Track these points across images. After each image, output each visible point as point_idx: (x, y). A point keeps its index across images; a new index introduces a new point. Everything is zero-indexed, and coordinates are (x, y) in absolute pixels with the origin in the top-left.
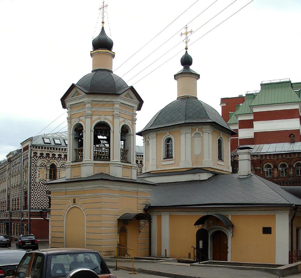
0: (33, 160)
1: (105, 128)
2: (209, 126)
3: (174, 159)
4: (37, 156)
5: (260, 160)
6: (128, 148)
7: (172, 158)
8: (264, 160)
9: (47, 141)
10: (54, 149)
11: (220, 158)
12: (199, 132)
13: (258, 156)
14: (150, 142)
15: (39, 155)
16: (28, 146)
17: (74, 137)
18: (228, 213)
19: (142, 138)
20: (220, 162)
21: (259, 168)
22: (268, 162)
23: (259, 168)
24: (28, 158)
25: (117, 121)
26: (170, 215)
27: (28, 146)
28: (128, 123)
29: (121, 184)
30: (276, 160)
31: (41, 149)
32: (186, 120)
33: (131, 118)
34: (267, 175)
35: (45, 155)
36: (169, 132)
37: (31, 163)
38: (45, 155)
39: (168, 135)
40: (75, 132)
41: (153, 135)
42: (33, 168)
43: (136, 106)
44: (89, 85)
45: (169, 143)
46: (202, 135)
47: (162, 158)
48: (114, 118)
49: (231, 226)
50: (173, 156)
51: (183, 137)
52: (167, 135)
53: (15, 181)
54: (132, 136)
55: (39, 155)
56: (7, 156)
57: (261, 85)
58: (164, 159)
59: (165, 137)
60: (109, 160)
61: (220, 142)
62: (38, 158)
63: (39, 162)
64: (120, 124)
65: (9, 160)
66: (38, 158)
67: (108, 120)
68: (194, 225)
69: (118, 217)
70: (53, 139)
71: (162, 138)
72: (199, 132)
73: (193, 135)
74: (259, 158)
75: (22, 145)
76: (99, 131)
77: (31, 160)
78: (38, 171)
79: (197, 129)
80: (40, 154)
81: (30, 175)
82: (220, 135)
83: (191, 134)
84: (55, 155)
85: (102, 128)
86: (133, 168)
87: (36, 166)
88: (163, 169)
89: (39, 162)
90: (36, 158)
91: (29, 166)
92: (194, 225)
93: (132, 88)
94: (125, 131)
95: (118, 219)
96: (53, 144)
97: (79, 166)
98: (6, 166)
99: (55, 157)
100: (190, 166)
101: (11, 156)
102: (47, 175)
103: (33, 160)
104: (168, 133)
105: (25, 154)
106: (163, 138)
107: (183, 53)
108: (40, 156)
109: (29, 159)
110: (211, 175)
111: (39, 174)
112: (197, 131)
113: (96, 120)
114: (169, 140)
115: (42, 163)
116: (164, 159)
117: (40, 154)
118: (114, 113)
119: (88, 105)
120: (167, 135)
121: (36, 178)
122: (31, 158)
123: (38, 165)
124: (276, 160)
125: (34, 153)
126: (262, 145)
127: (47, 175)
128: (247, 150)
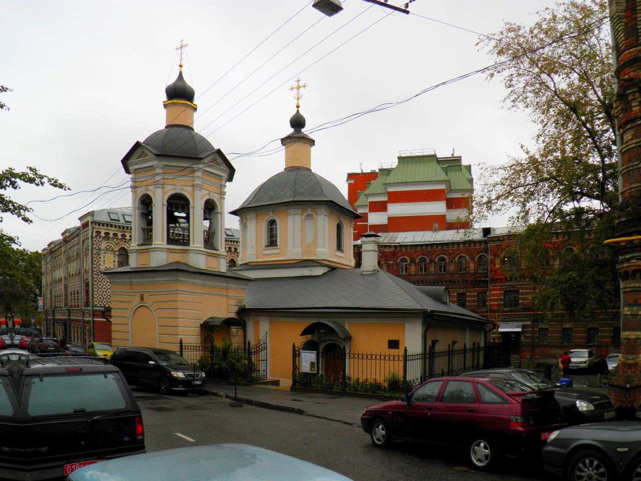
0: (95, 241)
1: (182, 202)
3: (279, 247)
4: (100, 236)
5: (394, 252)
6: (215, 230)
7: (276, 245)
9: (113, 216)
10: (123, 228)
14: (248, 224)
15: (103, 235)
16: (88, 222)
17: (140, 211)
19: (238, 218)
20: (339, 253)
21: (392, 262)
22: (404, 255)
23: (392, 262)
24: (88, 238)
25: (198, 193)
27: (88, 222)
28: (215, 198)
30: (413, 253)
31: (105, 227)
32: (296, 198)
33: (218, 190)
34: (402, 272)
35: (111, 235)
36: (273, 212)
37: (92, 244)
38: (111, 235)
39: (271, 215)
40: (141, 206)
41: (251, 216)
42: (95, 252)
43: (225, 176)
44: (160, 144)
45: (273, 227)
46: (315, 216)
47: (264, 246)
48: (194, 190)
50: (278, 243)
51: (290, 219)
52: (269, 216)
53: (73, 267)
54: (220, 215)
55: (103, 235)
56: (63, 234)
58: (266, 246)
59: (269, 218)
60: (188, 244)
61: (339, 227)
62: (101, 239)
63: (103, 244)
64: (203, 197)
65: (66, 240)
66: (101, 239)
67: (187, 192)
70: (123, 215)
71: (264, 219)
72: (312, 213)
73: (303, 217)
74: (392, 249)
75: (81, 221)
76: (174, 205)
77: (92, 241)
78: (102, 257)
79: (309, 210)
80: (105, 233)
81: (92, 261)
83: (302, 215)
84: (125, 236)
85: (178, 203)
86: (221, 256)
87: (99, 249)
88: (265, 260)
89: (104, 245)
90: (100, 238)
91: (90, 248)
93: (219, 152)
94: (210, 208)
96: (122, 221)
97: (147, 251)
98: (61, 247)
99: (126, 239)
100: (300, 257)
101: (68, 234)
102: (114, 261)
103: (95, 241)
104: (271, 213)
105: (84, 232)
106: (266, 219)
108: (104, 237)
109: (90, 239)
110: (327, 269)
111: (104, 260)
113: (170, 191)
114: (272, 223)
115: (108, 246)
116: (266, 246)
117: (105, 233)
118: (194, 183)
119: (158, 171)
120: (269, 216)
121: (100, 265)
122: (92, 238)
123: (102, 248)
125: (97, 232)
126: (397, 233)
127: (114, 261)
128: (373, 239)
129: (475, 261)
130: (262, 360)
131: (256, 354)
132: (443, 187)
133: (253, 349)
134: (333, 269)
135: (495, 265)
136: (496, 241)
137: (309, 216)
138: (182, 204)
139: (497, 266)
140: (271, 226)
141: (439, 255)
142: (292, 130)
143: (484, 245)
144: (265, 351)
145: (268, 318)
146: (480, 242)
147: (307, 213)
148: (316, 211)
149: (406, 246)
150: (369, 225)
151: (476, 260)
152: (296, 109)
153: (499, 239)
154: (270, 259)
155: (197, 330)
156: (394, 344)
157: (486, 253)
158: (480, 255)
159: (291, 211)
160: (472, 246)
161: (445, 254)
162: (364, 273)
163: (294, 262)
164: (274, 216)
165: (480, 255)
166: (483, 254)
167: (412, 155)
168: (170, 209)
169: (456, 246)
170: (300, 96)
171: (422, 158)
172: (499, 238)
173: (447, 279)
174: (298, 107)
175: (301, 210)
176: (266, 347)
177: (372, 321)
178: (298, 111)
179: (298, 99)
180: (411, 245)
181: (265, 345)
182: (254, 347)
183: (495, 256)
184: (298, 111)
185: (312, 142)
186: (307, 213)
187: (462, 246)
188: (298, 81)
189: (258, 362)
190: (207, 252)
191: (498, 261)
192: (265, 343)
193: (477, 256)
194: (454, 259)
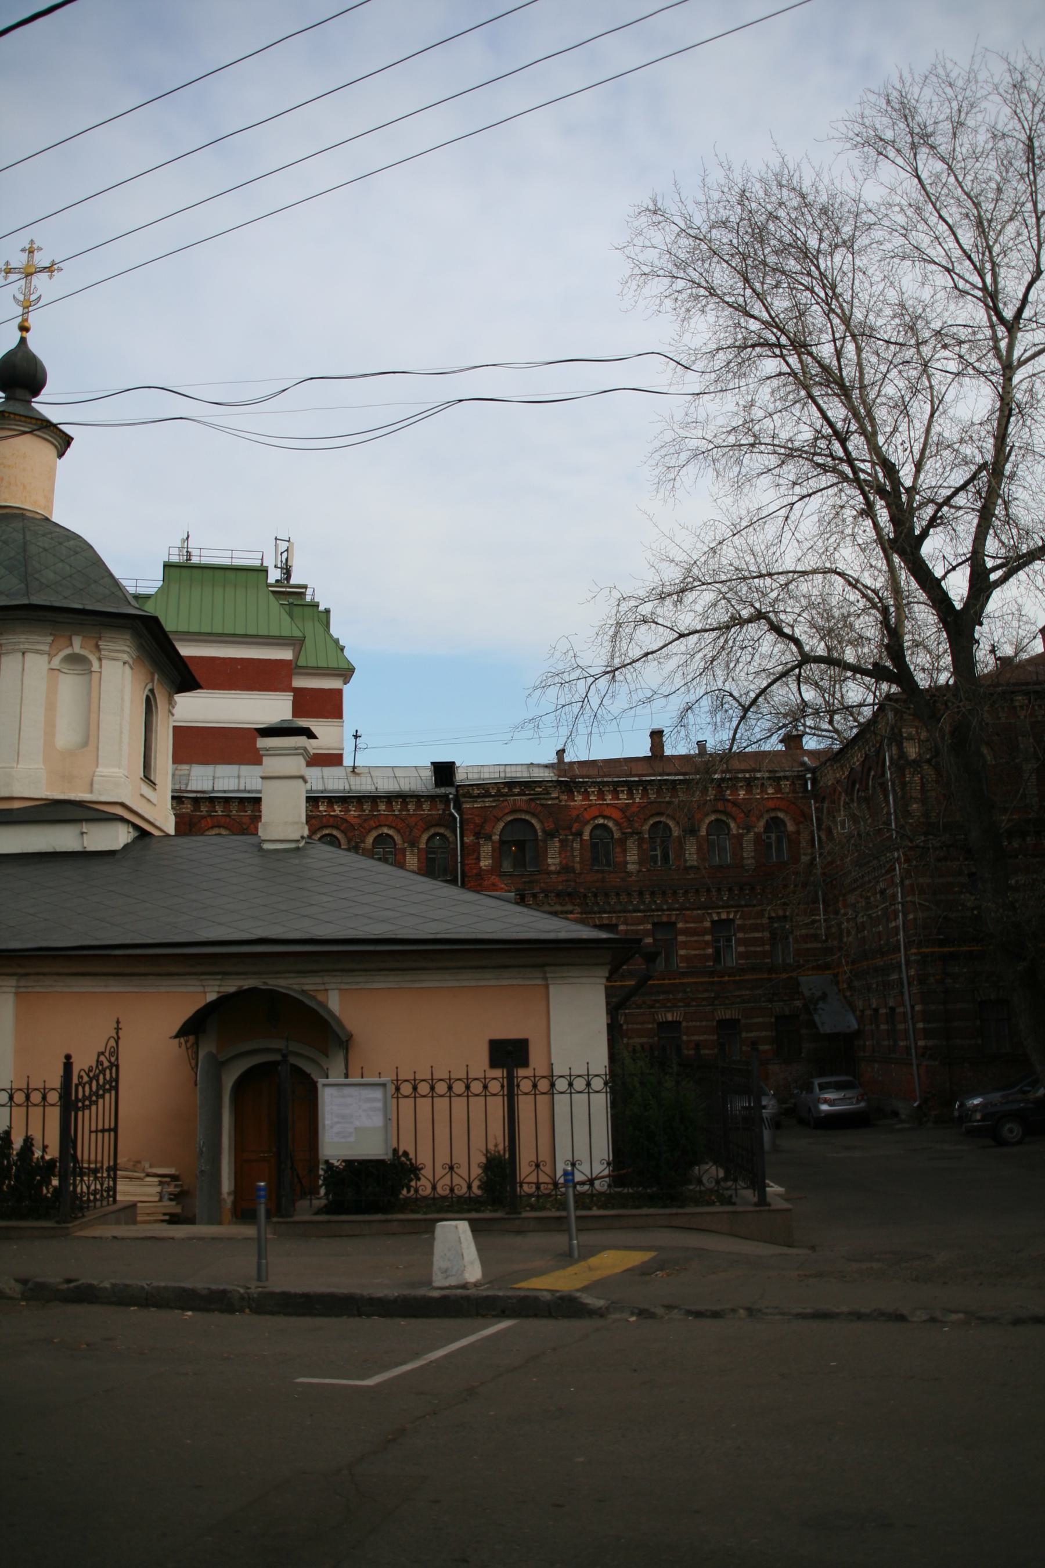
8: (203, 817)
12: (83, 652)
13: (183, 803)
18: (326, 979)
20: (146, 790)
22: (219, 827)
26: (17, 994)
30: (246, 820)
49: (329, 1037)
57: (165, 566)
68: (176, 1037)
73: (56, 662)
79: (77, 642)
82: (152, 681)
92: (176, 1037)
124: (246, 820)
128: (301, 741)
129: (419, 849)
130: (103, 1131)
131: (89, 1107)
132: (286, 654)
133: (80, 1089)
135: (478, 859)
136: (479, 796)
137: (76, 660)
139: (485, 863)
141: (326, 827)
143: (441, 806)
144: (113, 1092)
145: (12, 982)
146: (432, 798)
148: (97, 646)
149: (227, 800)
150: (339, 692)
151: (423, 846)
153: (483, 790)
156: (509, 1054)
157: (447, 827)
158: (432, 831)
159: (13, 638)
160: (411, 807)
161: (337, 828)
162: (266, 846)
163: (16, 805)
165: (432, 831)
166: (441, 830)
167: (237, 562)
169: (367, 806)
170: (33, 297)
171: (231, 575)
172: (487, 791)
174: (24, 328)
175: (50, 639)
176: (117, 1081)
177: (430, 981)
178: (23, 341)
180: (242, 800)
181: (114, 1069)
182: (86, 1079)
183: (477, 835)
184: (23, 341)
185: (63, 442)
187: (382, 807)
188: (31, 252)
189: (93, 1135)
191: (486, 849)
192: (112, 1065)
193: (425, 837)
194: (363, 842)
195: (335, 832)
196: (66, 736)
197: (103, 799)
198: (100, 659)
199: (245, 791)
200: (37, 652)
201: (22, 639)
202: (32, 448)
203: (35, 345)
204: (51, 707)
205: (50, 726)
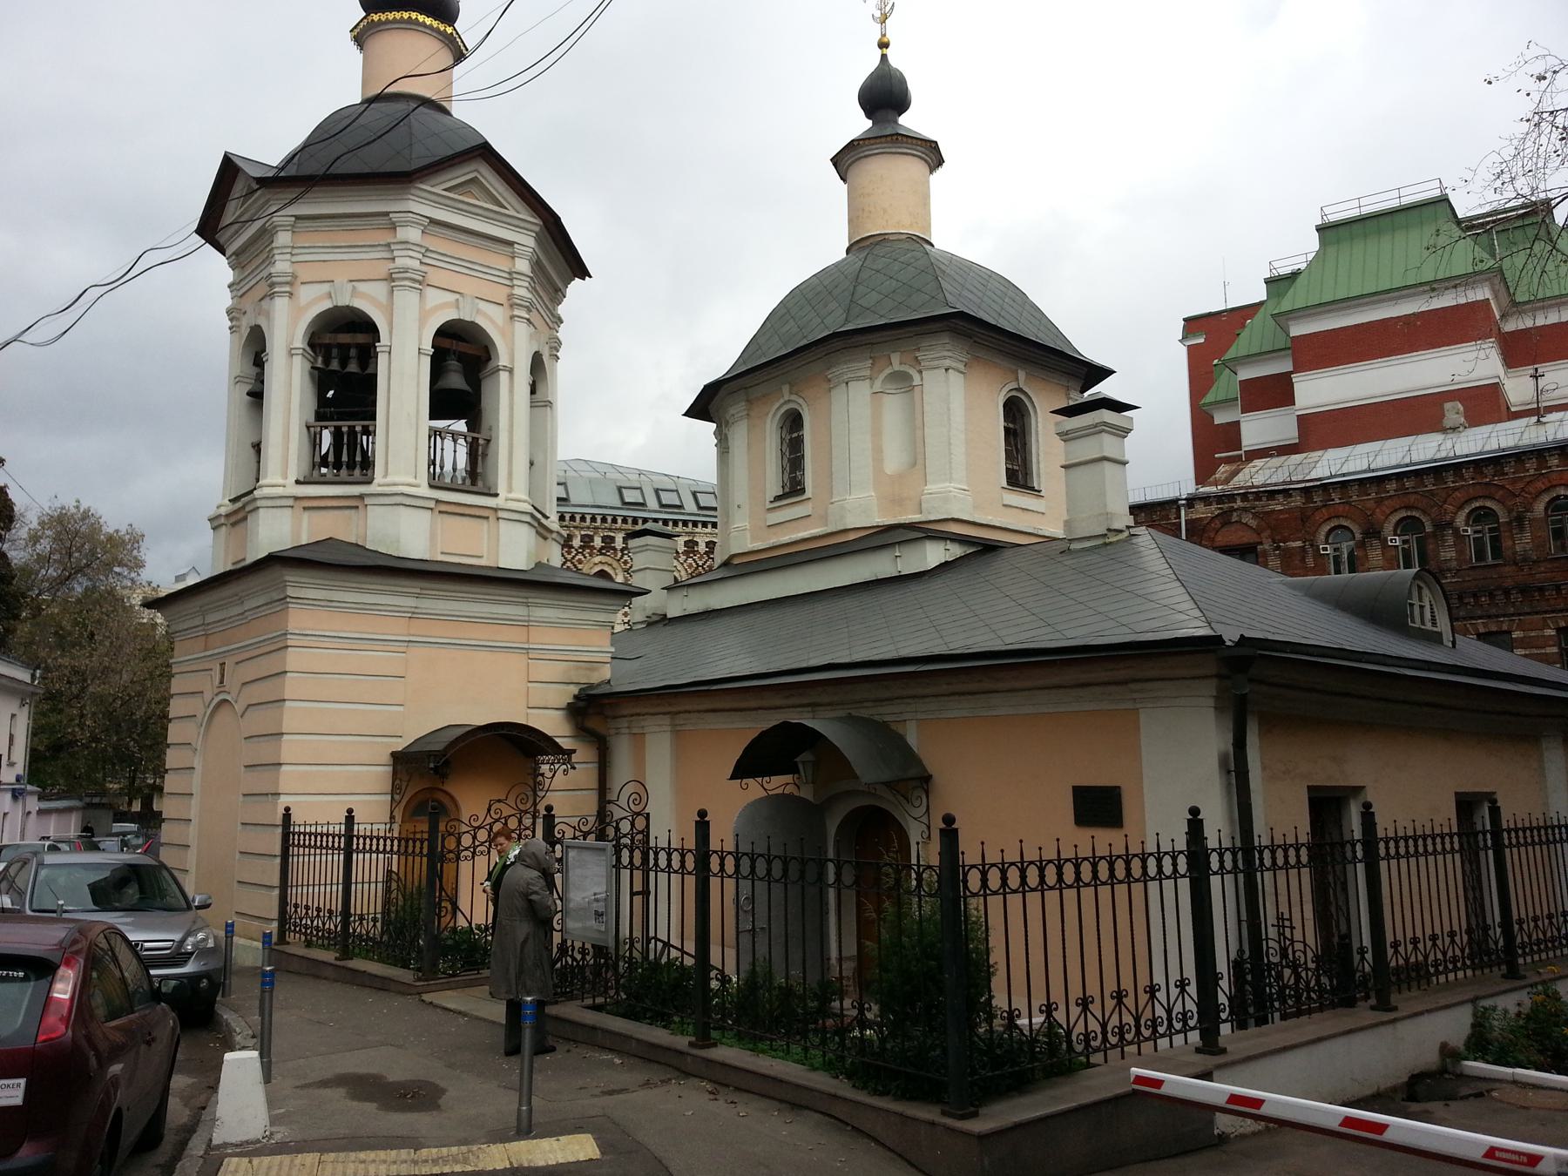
1: (361, 338)
2: (945, 339)
3: (809, 493)
11: (1019, 476)
23: (1299, 544)
29: (414, 586)
36: (791, 385)
46: (917, 381)
51: (838, 395)
54: (504, 376)
61: (1016, 413)
69: (400, 745)
73: (878, 386)
79: (895, 358)
95: (394, 754)
104: (786, 389)
107: (875, 62)
112: (897, 367)
114: (794, 422)
116: (778, 498)
134: (987, 549)
138: (358, 346)
140: (791, 432)
142: (869, 123)
147: (888, 371)
152: (879, 52)
154: (786, 539)
155: (380, 775)
163: (852, 536)
164: (793, 397)
168: (319, 364)
171: (1401, 216)
173: (1509, 583)
174: (883, 45)
178: (884, 57)
179: (884, 19)
184: (884, 57)
186: (888, 371)
190: (438, 501)
195: (1489, 504)
196: (894, 462)
197: (932, 518)
198: (920, 372)
199: (1412, 464)
200: (858, 379)
201: (843, 369)
202: (908, 167)
203: (895, 61)
204: (877, 433)
205: (878, 452)
